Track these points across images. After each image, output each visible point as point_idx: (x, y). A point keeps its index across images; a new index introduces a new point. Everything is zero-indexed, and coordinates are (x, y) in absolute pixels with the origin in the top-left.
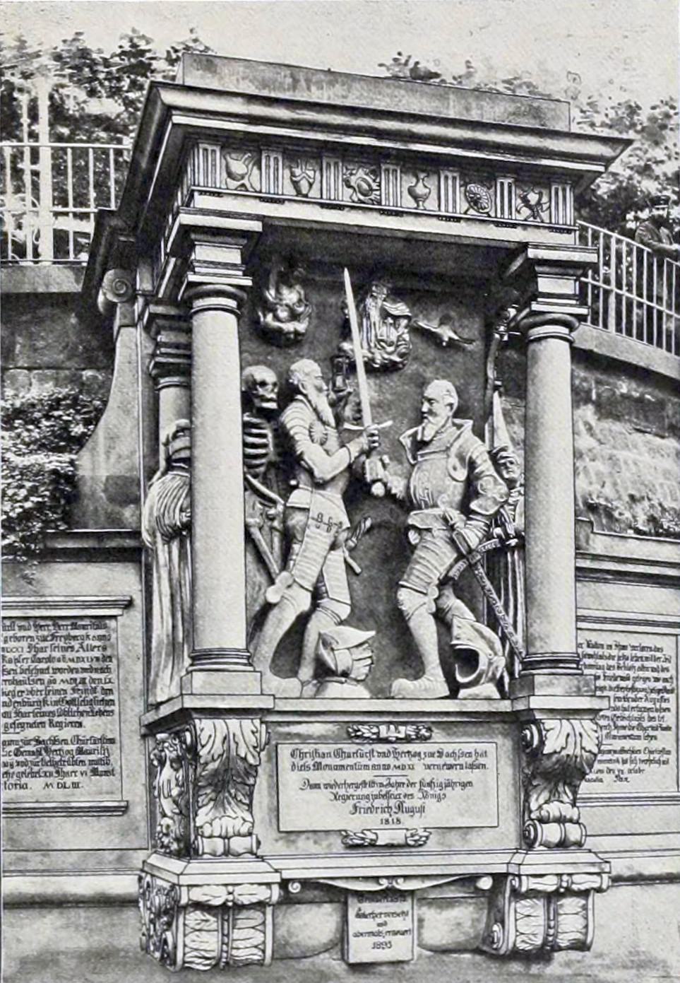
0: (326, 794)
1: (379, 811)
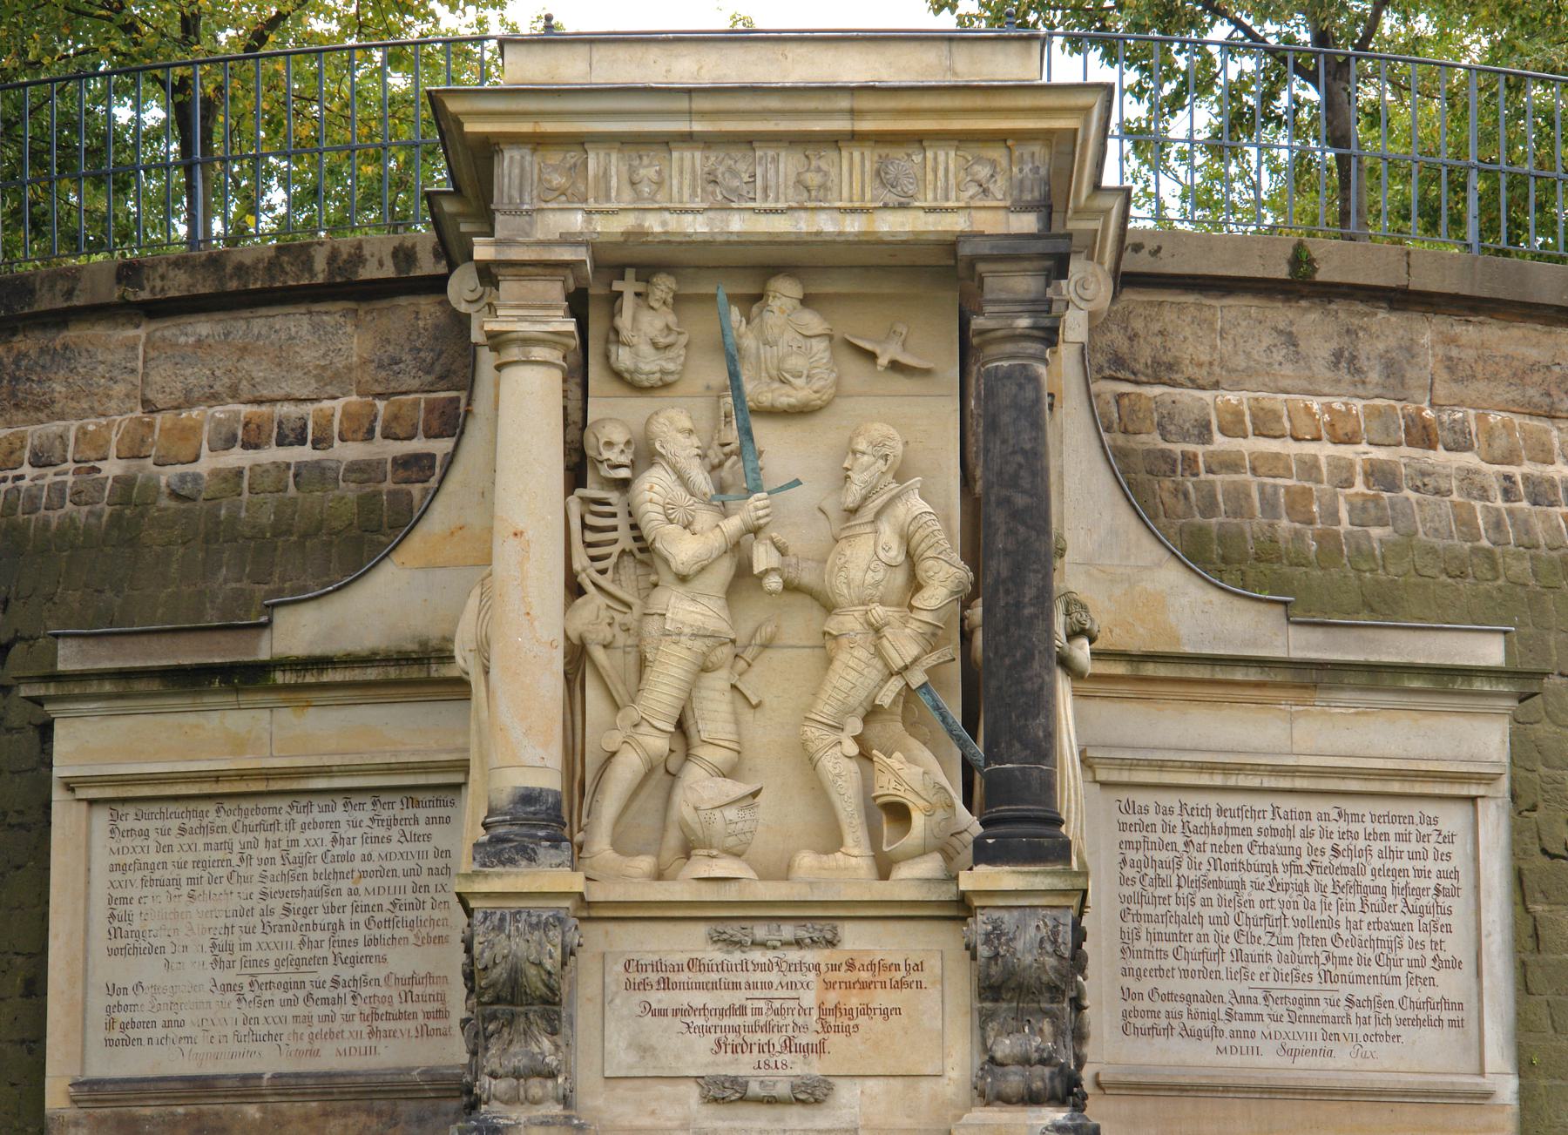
0: (678, 1023)
1: (755, 1049)
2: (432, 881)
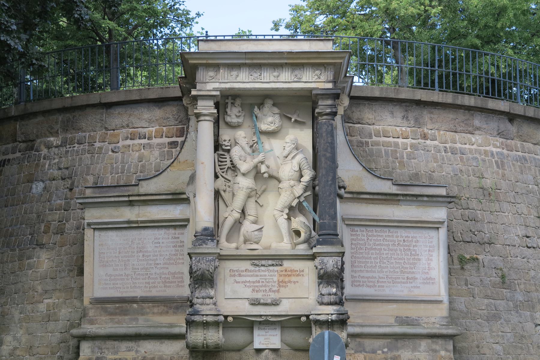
2: (179, 249)
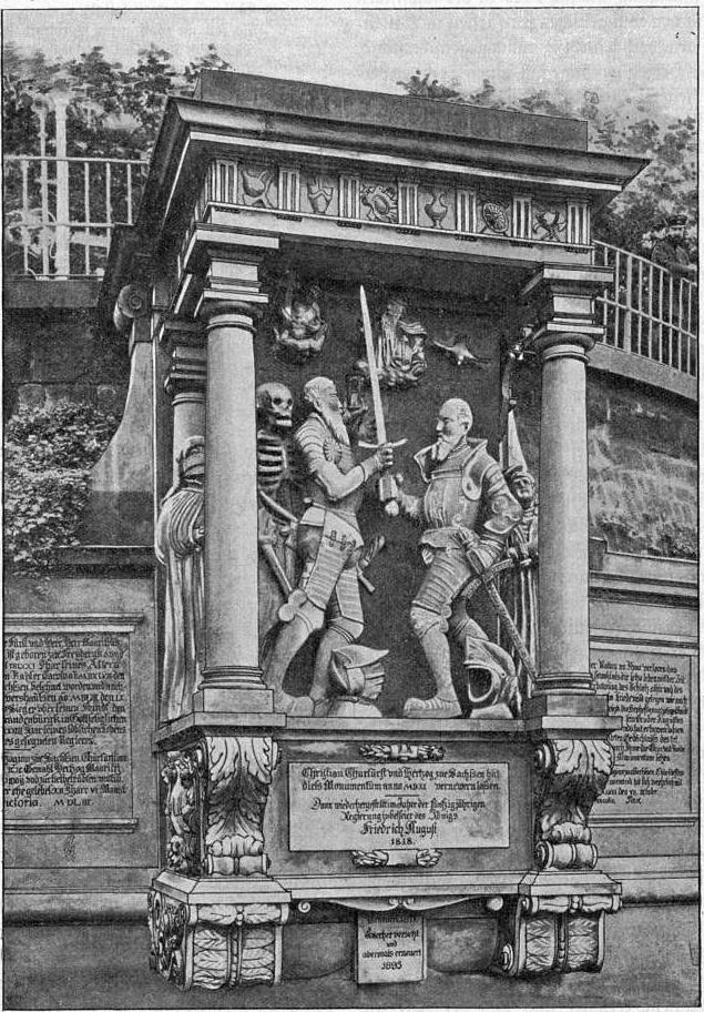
0: (340, 813)
1: (390, 830)
